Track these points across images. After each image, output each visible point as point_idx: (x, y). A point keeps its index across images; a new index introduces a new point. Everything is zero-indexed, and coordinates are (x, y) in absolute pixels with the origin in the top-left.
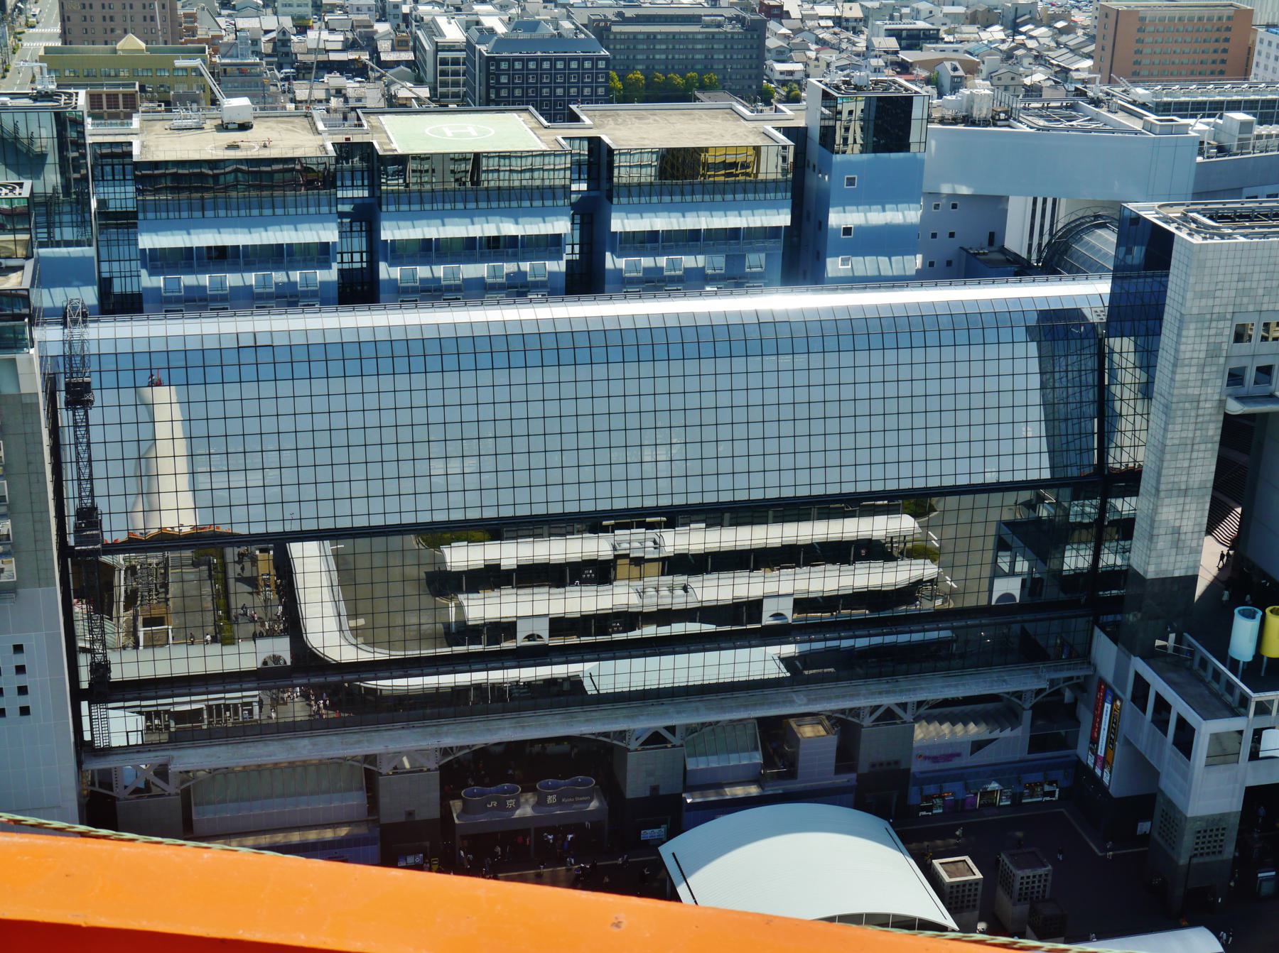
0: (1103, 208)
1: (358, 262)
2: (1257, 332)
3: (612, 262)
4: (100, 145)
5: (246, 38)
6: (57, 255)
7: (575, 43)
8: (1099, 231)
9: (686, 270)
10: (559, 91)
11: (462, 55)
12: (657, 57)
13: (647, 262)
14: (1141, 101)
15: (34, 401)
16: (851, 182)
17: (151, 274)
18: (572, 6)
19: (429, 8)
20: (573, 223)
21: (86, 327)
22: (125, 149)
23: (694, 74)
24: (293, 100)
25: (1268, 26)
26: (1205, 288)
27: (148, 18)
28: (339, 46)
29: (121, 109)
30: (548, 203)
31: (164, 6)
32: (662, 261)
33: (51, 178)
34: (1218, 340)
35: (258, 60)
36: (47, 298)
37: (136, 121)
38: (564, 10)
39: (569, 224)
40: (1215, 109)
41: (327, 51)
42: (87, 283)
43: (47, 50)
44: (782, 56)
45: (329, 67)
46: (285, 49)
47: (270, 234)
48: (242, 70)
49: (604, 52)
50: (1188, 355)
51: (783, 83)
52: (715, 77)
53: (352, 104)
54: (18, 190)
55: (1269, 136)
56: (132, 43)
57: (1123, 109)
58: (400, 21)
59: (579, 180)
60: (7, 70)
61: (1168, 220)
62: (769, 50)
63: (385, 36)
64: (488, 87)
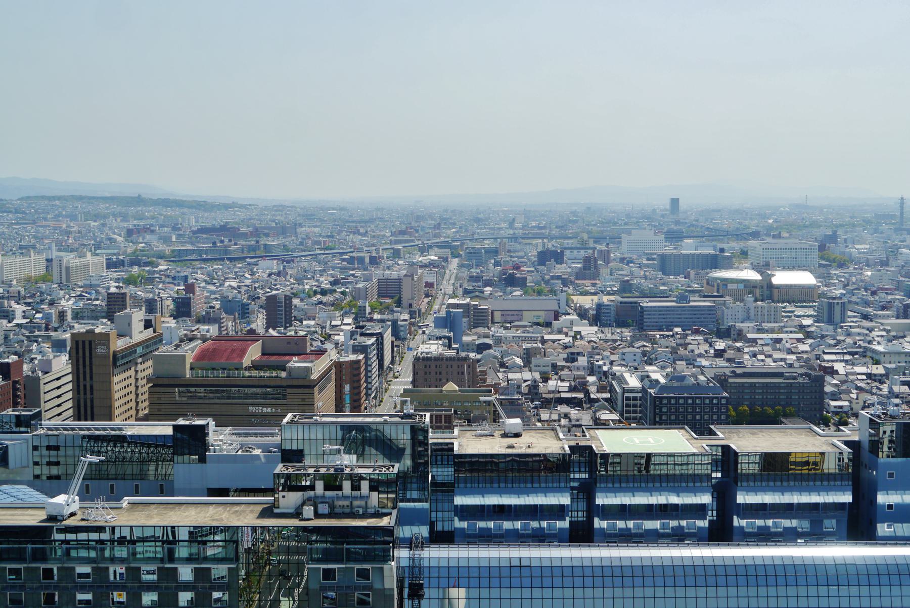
1: (581, 516)
3: (736, 522)
4: (436, 444)
5: (514, 384)
6: (408, 507)
7: (706, 389)
9: (785, 528)
10: (698, 417)
11: (640, 395)
12: (757, 397)
13: (760, 522)
15: (392, 593)
16: (891, 475)
17: (460, 520)
18: (704, 367)
19: (619, 368)
20: (713, 497)
21: (423, 550)
22: (450, 446)
23: (780, 407)
24: (540, 421)
27: (460, 373)
28: (566, 389)
29: (443, 423)
30: (698, 484)
31: (469, 367)
32: (770, 522)
33: (408, 462)
35: (520, 397)
36: (406, 532)
37: (456, 431)
38: (699, 369)
39: (711, 498)
41: (560, 392)
42: (423, 524)
43: (405, 390)
44: (835, 397)
45: (561, 401)
46: (536, 391)
47: (531, 498)
48: (512, 403)
49: (725, 394)
51: (836, 413)
52: (793, 409)
53: (574, 423)
54: (391, 469)
56: (452, 386)
58: (602, 375)
59: (717, 471)
60: (381, 401)
62: (826, 393)
63: (593, 384)
64: (655, 414)
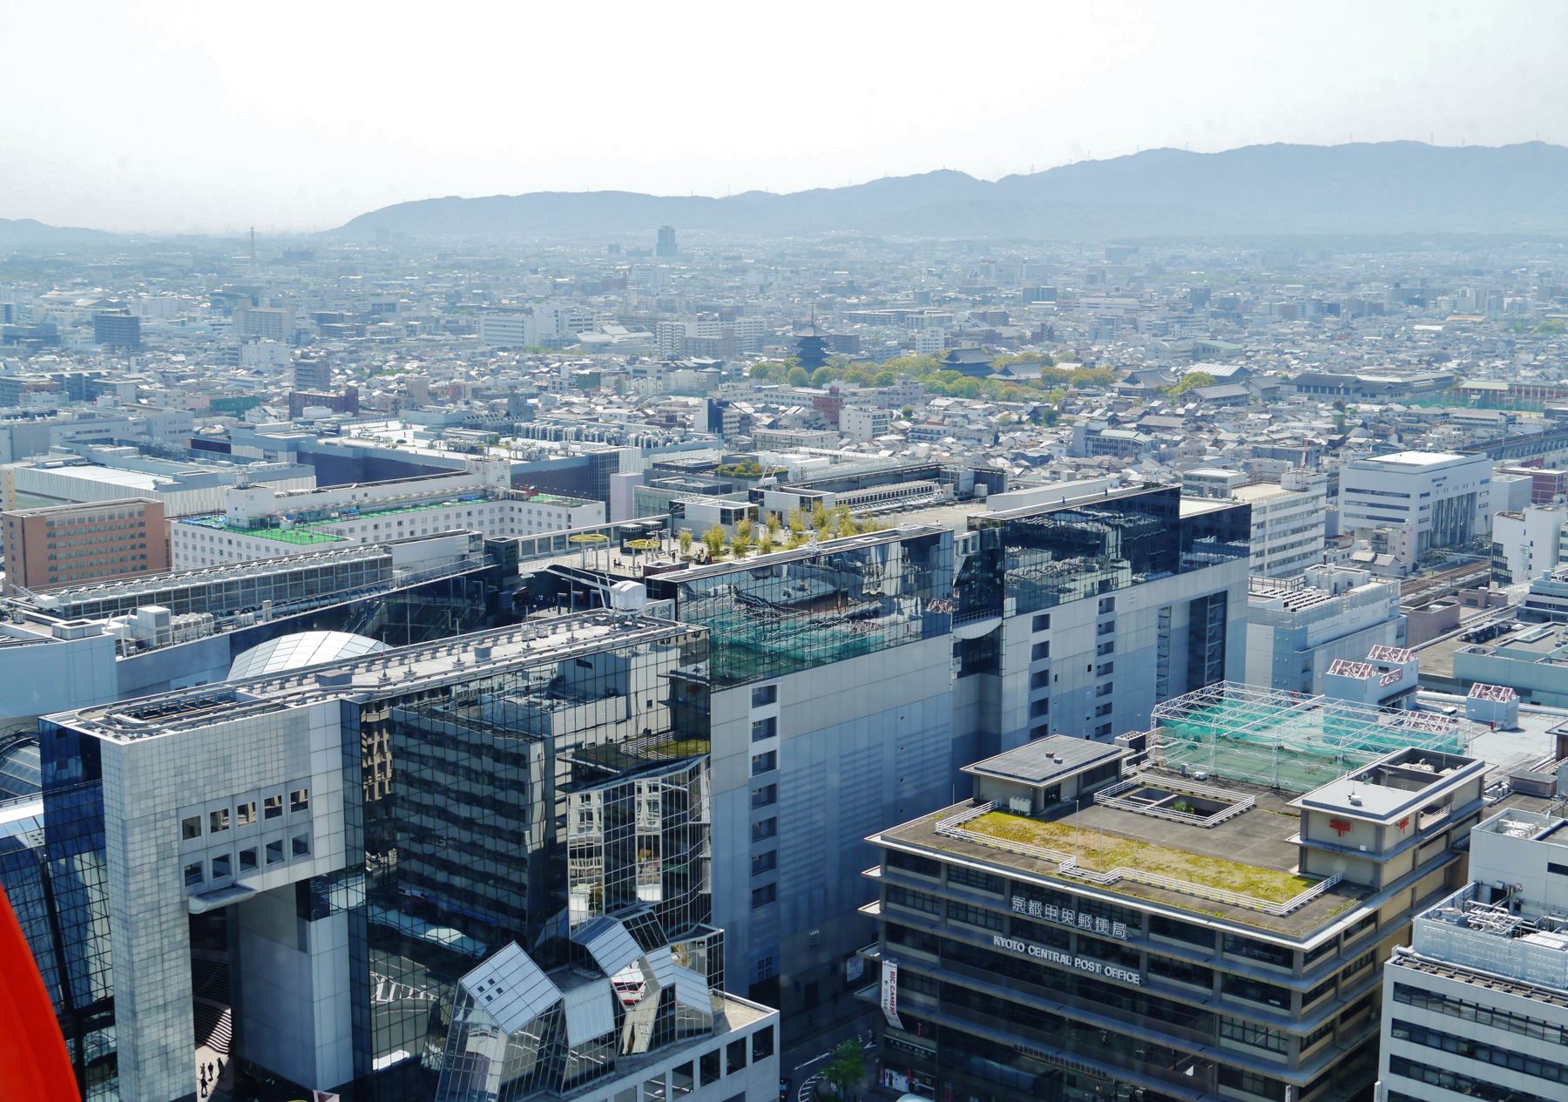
0: (25, 724)
2: (206, 824)
8: (23, 750)
14: (47, 607)
25: (180, 517)
26: (143, 788)
34: (167, 839)
40: (130, 604)
50: (138, 862)
55: (187, 625)
57: (29, 618)
61: (90, 726)
